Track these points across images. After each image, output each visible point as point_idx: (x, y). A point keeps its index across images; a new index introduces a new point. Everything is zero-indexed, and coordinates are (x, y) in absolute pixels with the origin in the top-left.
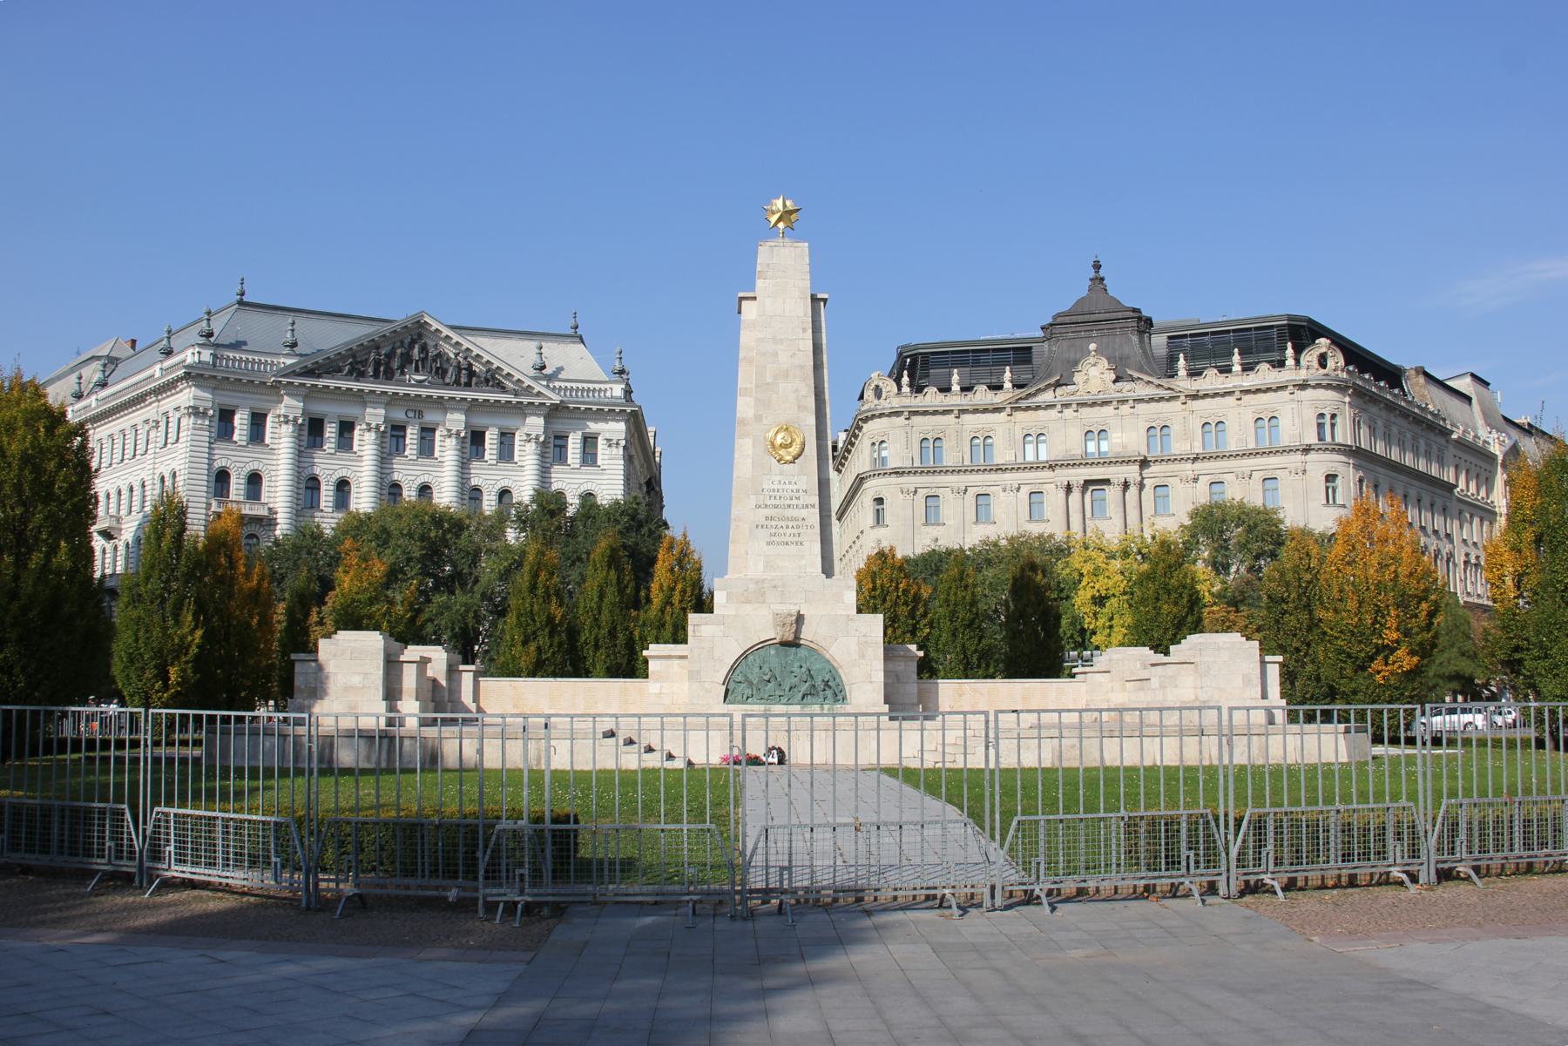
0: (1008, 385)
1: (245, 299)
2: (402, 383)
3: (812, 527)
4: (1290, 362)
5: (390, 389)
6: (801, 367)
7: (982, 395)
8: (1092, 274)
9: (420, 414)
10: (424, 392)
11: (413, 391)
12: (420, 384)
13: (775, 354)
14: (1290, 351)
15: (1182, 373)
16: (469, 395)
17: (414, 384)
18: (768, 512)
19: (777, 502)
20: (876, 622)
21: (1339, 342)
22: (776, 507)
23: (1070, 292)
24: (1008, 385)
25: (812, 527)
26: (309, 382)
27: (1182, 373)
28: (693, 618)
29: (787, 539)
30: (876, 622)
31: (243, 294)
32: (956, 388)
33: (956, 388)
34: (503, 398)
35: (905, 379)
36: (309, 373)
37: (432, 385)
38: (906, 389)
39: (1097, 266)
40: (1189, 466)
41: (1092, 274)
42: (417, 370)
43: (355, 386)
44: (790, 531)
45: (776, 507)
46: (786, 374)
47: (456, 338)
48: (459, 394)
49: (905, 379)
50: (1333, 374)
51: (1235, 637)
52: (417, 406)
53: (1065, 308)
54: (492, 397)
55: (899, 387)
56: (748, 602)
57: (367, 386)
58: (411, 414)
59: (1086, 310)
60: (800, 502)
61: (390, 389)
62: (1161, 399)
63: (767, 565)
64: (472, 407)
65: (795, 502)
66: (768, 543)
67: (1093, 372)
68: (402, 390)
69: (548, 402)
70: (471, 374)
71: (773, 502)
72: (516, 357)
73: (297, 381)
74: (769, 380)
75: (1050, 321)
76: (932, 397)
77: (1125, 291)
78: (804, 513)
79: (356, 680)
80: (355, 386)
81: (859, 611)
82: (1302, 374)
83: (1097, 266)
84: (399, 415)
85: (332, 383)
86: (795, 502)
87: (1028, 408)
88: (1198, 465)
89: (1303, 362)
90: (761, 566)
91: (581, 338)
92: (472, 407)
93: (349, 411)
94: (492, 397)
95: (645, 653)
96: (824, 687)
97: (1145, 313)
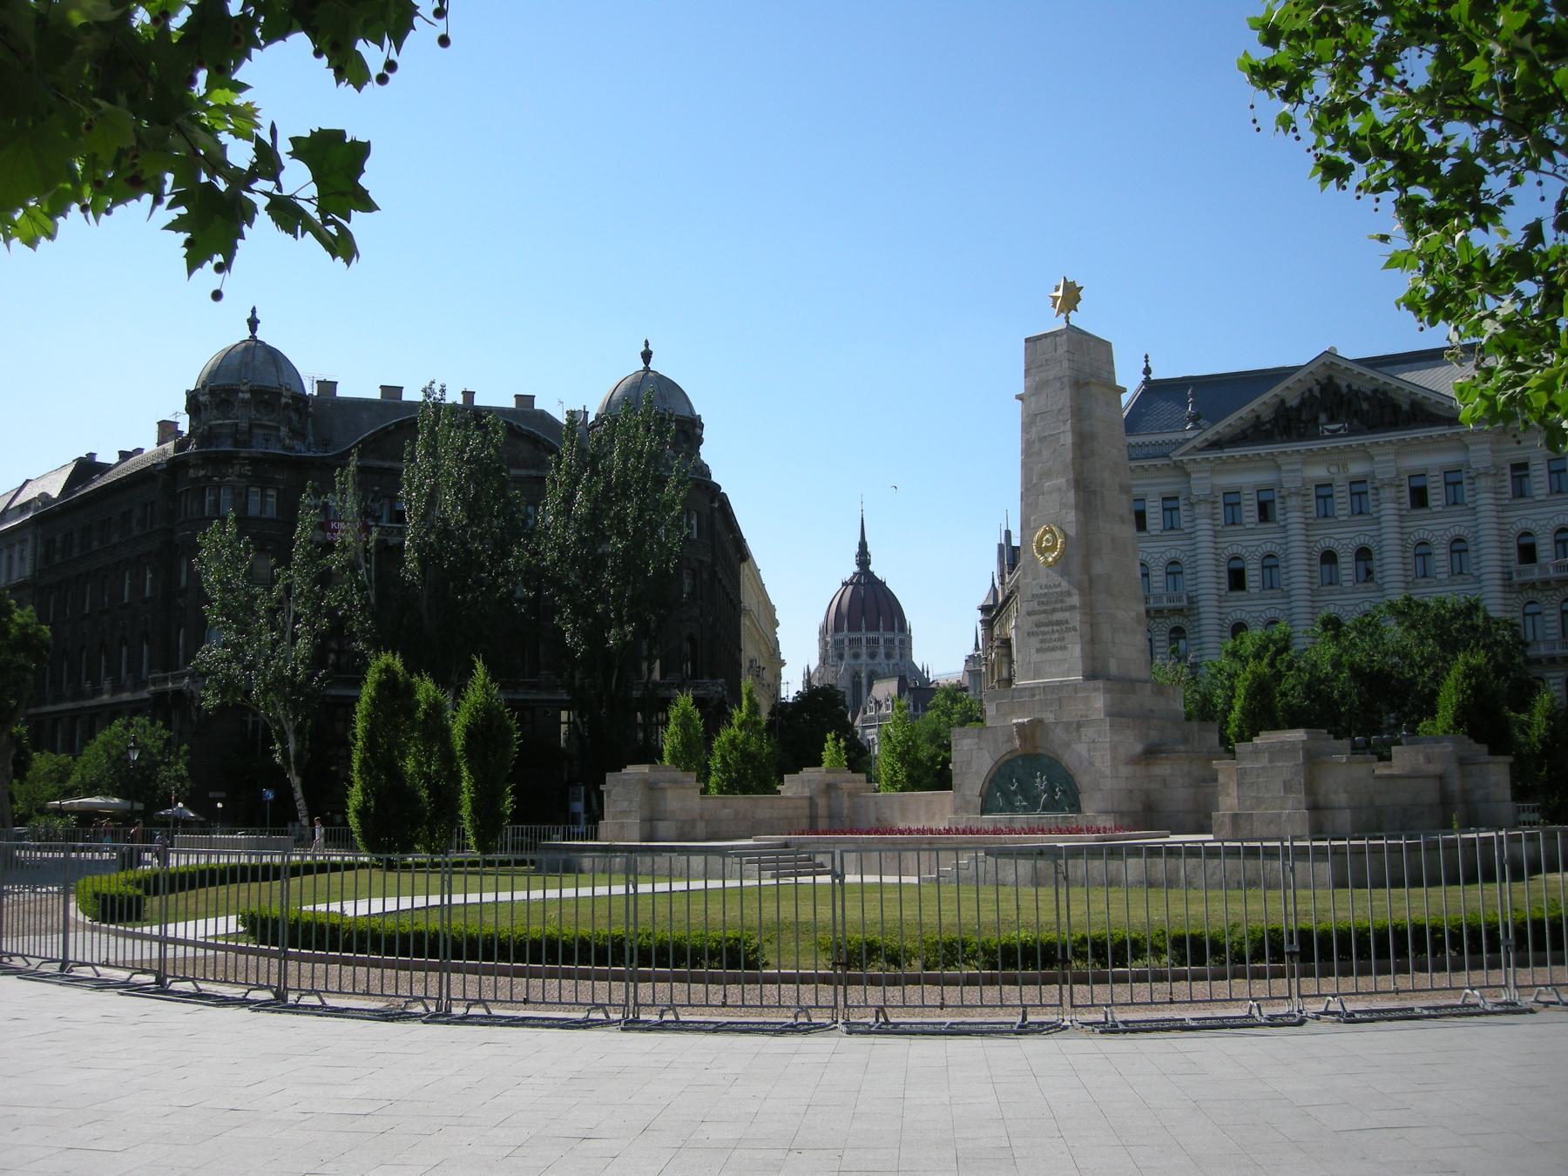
1: (1153, 377)
2: (1316, 436)
5: (1302, 446)
9: (1345, 466)
12: (1334, 434)
16: (1394, 436)
18: (1035, 618)
22: (1045, 612)
25: (1074, 629)
26: (1211, 455)
31: (1147, 371)
37: (1353, 432)
42: (1332, 420)
44: (1056, 636)
45: (1045, 612)
47: (1370, 373)
54: (1421, 433)
57: (1275, 448)
65: (1058, 606)
66: (1038, 651)
70: (1396, 408)
73: (1198, 457)
78: (1067, 615)
80: (1263, 450)
84: (1319, 472)
85: (1238, 452)
86: (1058, 606)
96: (1065, 795)
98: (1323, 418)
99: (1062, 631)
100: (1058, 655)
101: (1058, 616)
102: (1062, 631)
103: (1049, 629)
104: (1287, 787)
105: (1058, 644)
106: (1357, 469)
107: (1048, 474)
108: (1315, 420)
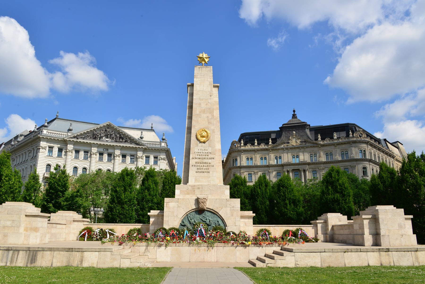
0: (270, 143)
1: (59, 117)
2: (103, 141)
3: (213, 166)
4: (351, 136)
6: (209, 109)
7: (263, 146)
8: (293, 113)
9: (108, 149)
10: (109, 144)
11: (105, 143)
13: (200, 104)
14: (350, 132)
15: (320, 139)
16: (122, 145)
17: (106, 141)
19: (200, 157)
20: (237, 202)
21: (364, 131)
22: (199, 158)
23: (286, 119)
24: (270, 143)
27: (320, 139)
28: (166, 200)
29: (203, 171)
30: (237, 202)
32: (256, 144)
33: (256, 144)
34: (131, 146)
35: (242, 142)
36: (74, 137)
37: (112, 142)
38: (242, 144)
39: (294, 111)
40: (322, 165)
41: (293, 113)
42: (107, 138)
43: (89, 141)
45: (199, 158)
46: (204, 111)
48: (118, 144)
49: (242, 142)
50: (363, 139)
51: (392, 207)
52: (107, 147)
53: (286, 122)
54: (128, 145)
55: (241, 144)
56: (188, 194)
58: (105, 150)
59: (292, 123)
60: (209, 157)
61: (99, 143)
62: (314, 147)
63: (196, 180)
64: (122, 148)
65: (207, 157)
66: (196, 172)
67: (294, 140)
68: (102, 143)
69: (144, 147)
71: (198, 157)
72: (135, 134)
73: (71, 140)
74: (198, 113)
75: (282, 126)
76: (249, 147)
77: (302, 118)
78: (210, 161)
79: (9, 223)
81: (230, 198)
82: (355, 139)
83: (294, 111)
84: (101, 150)
86: (207, 157)
87: (276, 149)
88: (325, 165)
89: (354, 135)
90: (194, 180)
91: (153, 130)
92: (122, 148)
93: (87, 149)
94: (128, 145)
95: (149, 214)
97: (308, 123)
98: (104, 138)
99: (208, 166)
100: (206, 174)
101: (205, 161)
102: (208, 166)
103: (202, 165)
104: (401, 226)
105: (205, 170)
106: (110, 151)
107: (204, 111)
108: (101, 137)
